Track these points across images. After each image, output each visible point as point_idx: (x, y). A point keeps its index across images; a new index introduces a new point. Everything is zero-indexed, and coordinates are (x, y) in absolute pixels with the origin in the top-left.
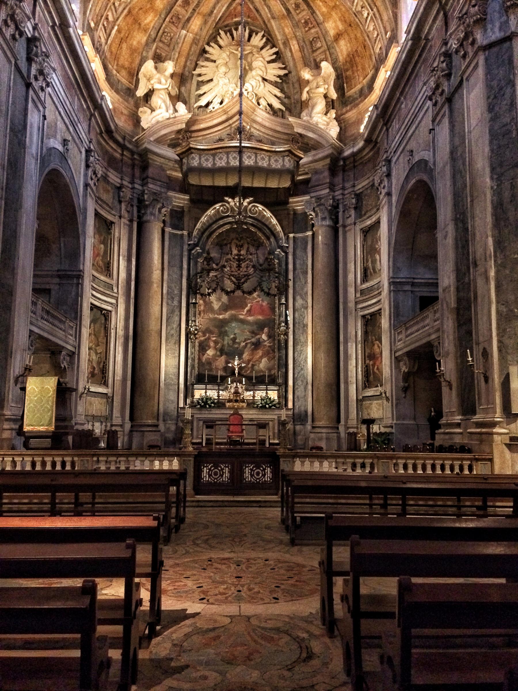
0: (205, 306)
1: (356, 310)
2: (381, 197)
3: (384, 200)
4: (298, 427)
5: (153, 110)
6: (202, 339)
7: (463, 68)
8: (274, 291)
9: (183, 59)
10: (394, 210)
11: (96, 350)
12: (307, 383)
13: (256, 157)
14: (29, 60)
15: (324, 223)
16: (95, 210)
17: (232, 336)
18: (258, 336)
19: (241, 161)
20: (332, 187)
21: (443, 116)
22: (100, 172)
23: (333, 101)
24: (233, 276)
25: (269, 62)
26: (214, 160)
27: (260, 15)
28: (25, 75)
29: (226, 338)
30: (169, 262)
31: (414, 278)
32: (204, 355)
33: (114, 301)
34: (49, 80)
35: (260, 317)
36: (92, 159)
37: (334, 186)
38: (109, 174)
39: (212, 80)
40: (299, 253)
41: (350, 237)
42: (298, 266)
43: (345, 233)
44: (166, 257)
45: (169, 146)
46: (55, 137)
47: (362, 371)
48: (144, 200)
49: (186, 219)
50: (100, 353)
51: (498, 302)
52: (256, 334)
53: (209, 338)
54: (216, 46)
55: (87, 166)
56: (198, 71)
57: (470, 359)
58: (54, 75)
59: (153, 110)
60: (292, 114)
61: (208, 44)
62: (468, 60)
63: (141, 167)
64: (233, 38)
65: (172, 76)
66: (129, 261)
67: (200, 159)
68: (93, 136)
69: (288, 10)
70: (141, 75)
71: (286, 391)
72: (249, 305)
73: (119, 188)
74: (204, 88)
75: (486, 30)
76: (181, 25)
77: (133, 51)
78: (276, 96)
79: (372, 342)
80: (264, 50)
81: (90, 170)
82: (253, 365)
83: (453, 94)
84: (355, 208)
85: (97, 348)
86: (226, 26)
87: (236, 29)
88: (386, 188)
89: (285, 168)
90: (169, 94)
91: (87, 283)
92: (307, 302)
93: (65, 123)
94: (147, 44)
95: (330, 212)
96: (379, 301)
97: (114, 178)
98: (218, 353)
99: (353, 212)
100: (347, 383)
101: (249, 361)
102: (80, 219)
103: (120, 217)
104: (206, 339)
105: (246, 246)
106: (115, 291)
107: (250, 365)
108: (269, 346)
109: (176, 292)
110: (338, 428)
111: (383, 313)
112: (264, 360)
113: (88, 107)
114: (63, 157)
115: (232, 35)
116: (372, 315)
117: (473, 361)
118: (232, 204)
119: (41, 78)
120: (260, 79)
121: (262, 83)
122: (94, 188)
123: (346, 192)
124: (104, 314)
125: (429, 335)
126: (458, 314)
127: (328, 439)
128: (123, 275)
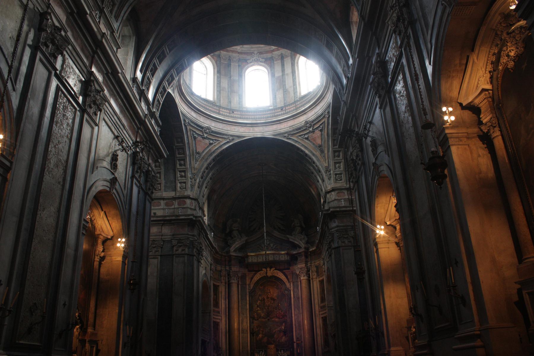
1: (319, 315)
6: (257, 330)
17: (269, 328)
18: (281, 327)
30: (241, 298)
33: (220, 318)
36: (212, 267)
37: (307, 262)
41: (315, 283)
42: (295, 296)
43: (313, 282)
44: (240, 296)
49: (247, 279)
55: (211, 270)
59: (232, 238)
67: (252, 259)
73: (221, 271)
82: (279, 340)
95: (307, 274)
96: (326, 312)
97: (219, 268)
99: (315, 273)
100: (317, 346)
103: (221, 283)
107: (278, 340)
113: (211, 249)
128: (223, 306)
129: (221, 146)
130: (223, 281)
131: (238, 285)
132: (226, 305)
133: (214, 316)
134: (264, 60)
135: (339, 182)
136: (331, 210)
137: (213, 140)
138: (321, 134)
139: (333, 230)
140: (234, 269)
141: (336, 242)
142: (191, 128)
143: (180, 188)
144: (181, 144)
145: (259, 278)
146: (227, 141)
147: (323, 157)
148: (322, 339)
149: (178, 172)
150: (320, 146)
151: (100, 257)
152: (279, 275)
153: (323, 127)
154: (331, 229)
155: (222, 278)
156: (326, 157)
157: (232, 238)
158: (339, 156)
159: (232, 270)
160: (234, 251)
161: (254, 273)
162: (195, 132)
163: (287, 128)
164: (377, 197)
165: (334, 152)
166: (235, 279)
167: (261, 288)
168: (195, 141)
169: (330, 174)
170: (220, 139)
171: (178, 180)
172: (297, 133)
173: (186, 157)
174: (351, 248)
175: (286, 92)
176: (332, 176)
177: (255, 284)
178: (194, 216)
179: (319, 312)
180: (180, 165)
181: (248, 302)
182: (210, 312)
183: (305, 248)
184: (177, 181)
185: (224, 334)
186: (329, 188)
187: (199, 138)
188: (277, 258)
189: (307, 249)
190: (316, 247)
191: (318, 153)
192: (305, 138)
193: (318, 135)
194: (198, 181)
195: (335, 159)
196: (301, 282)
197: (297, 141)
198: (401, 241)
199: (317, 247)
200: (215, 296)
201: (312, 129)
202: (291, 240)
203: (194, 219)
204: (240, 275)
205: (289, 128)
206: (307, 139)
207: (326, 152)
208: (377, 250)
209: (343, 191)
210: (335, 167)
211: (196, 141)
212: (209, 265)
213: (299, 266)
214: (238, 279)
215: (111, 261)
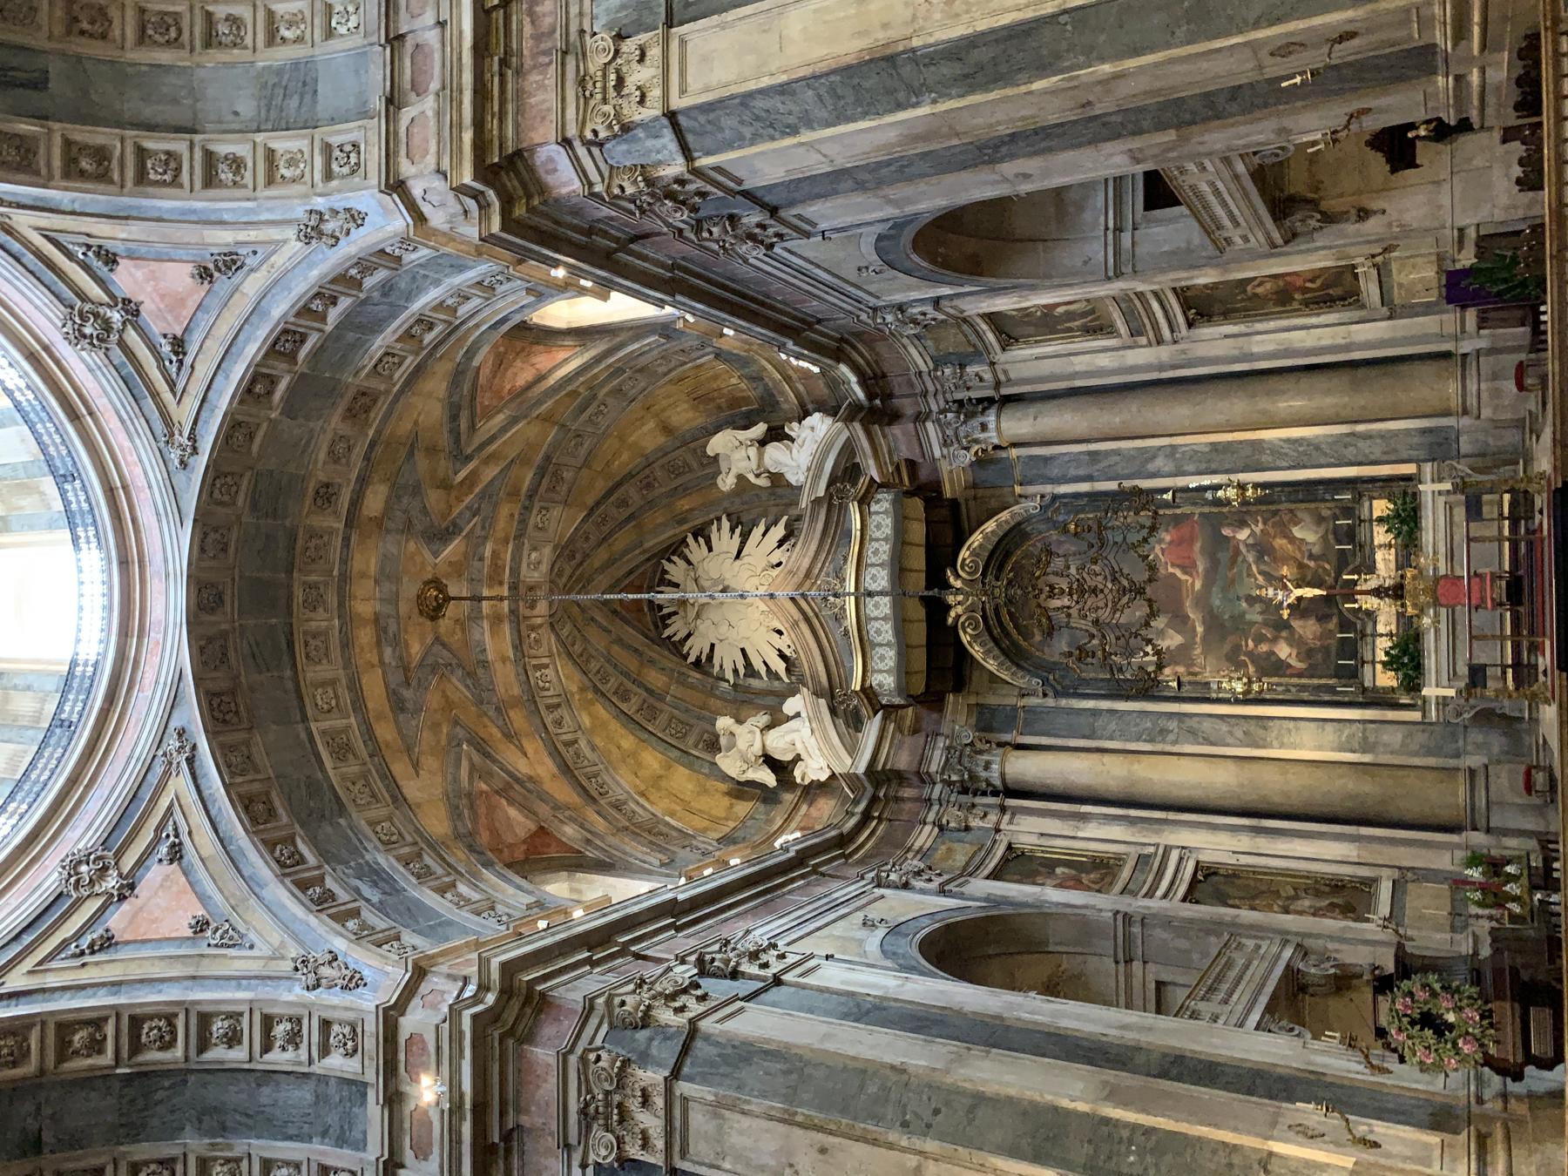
0: (1177, 663)
2: (941, 317)
4: (1465, 446)
5: (798, 758)
6: (1251, 669)
7: (721, 194)
8: (1145, 517)
9: (712, 701)
10: (967, 289)
11: (1288, 898)
12: (1353, 434)
13: (873, 565)
14: (735, 974)
15: (992, 426)
16: (987, 878)
18: (1243, 548)
19: (881, 593)
20: (920, 418)
21: (799, 217)
22: (915, 862)
23: (769, 429)
24: (1115, 604)
25: (710, 550)
26: (881, 645)
27: (637, 567)
28: (762, 984)
29: (1248, 617)
30: (1084, 737)
31: (1107, 229)
32: (1289, 666)
33: (1175, 855)
34: (766, 944)
35: (1197, 546)
36: (893, 877)
38: (917, 845)
39: (743, 650)
40: (1055, 472)
42: (1081, 472)
45: (858, 730)
46: (861, 942)
47: (1318, 315)
48: (962, 782)
49: (992, 700)
51: (1168, 46)
52: (1237, 552)
53: (1250, 654)
54: (689, 643)
55: (906, 886)
56: (729, 675)
57: (1298, 80)
58: (757, 933)
60: (795, 503)
61: (685, 657)
62: (709, 188)
63: (900, 785)
64: (675, 613)
65: (740, 722)
66: (1084, 817)
67: (881, 671)
68: (853, 872)
70: (743, 778)
71: (1373, 480)
72: (1171, 570)
73: (941, 828)
75: (660, 163)
76: (658, 705)
77: (704, 791)
78: (764, 535)
79: (1249, 299)
80: (690, 557)
81: (914, 882)
83: (763, 205)
84: (962, 366)
85: (1283, 894)
86: (657, 627)
87: (660, 608)
88: (923, 309)
90: (769, 727)
91: (1138, 905)
92: (1160, 448)
93: (834, 921)
94: (690, 767)
95: (970, 416)
96: (1155, 294)
97: (924, 836)
98: (1284, 634)
99: (971, 370)
100: (1348, 348)
102: (1009, 910)
103: (998, 831)
104: (1253, 662)
105: (1053, 579)
106: (1152, 850)
108: (1265, 523)
109: (1149, 725)
110: (1465, 356)
111: (1183, 284)
112: (1297, 532)
113: (802, 877)
114: (895, 930)
115: (670, 615)
116: (1186, 305)
117: (1300, 74)
118: (960, 609)
119: (764, 958)
120: (738, 562)
122: (946, 877)
123: (931, 388)
124: (1206, 877)
125: (1236, 177)
126: (1194, 123)
127: (1495, 377)
128: (1116, 832)
133: (1159, 893)
136: (467, 178)
137: (157, 840)
138: (131, 256)
139: (594, 176)
141: (650, 143)
142: (29, 963)
143: (350, 1054)
144: (110, 1030)
146: (184, 765)
147: (259, 257)
148: (1314, 320)
149: (268, 1057)
150: (204, 274)
153: (79, 245)
154: (591, 185)
155: (975, 823)
156: (252, 235)
157: (798, 758)
158: (237, 164)
162: (65, 944)
163: (136, 448)
165: (210, 180)
166: (986, 757)
168: (127, 943)
169: (335, 212)
170: (164, 803)
171: (310, 1062)
172: (155, 395)
173: (187, 1006)
174: (674, 45)
176: (338, 201)
178: (476, 999)
179: (1160, 341)
180: (233, 1039)
181: (1105, 704)
182: (1128, 918)
183: (849, 420)
184: (317, 1068)
185: (1264, 844)
187: (117, 920)
188: (880, 551)
189: (854, 413)
190: (838, 360)
191: (252, 285)
192: (176, 353)
193: (139, 274)
194: (340, 944)
195: (251, 186)
197: (203, 400)
199: (839, 355)
200: (1059, 870)
201: (109, 306)
202: (821, 493)
203: (490, 999)
204: (968, 735)
205: (137, 441)
206: (179, 345)
207: (224, 238)
211: (128, 937)
212: (882, 891)
213: (937, 454)
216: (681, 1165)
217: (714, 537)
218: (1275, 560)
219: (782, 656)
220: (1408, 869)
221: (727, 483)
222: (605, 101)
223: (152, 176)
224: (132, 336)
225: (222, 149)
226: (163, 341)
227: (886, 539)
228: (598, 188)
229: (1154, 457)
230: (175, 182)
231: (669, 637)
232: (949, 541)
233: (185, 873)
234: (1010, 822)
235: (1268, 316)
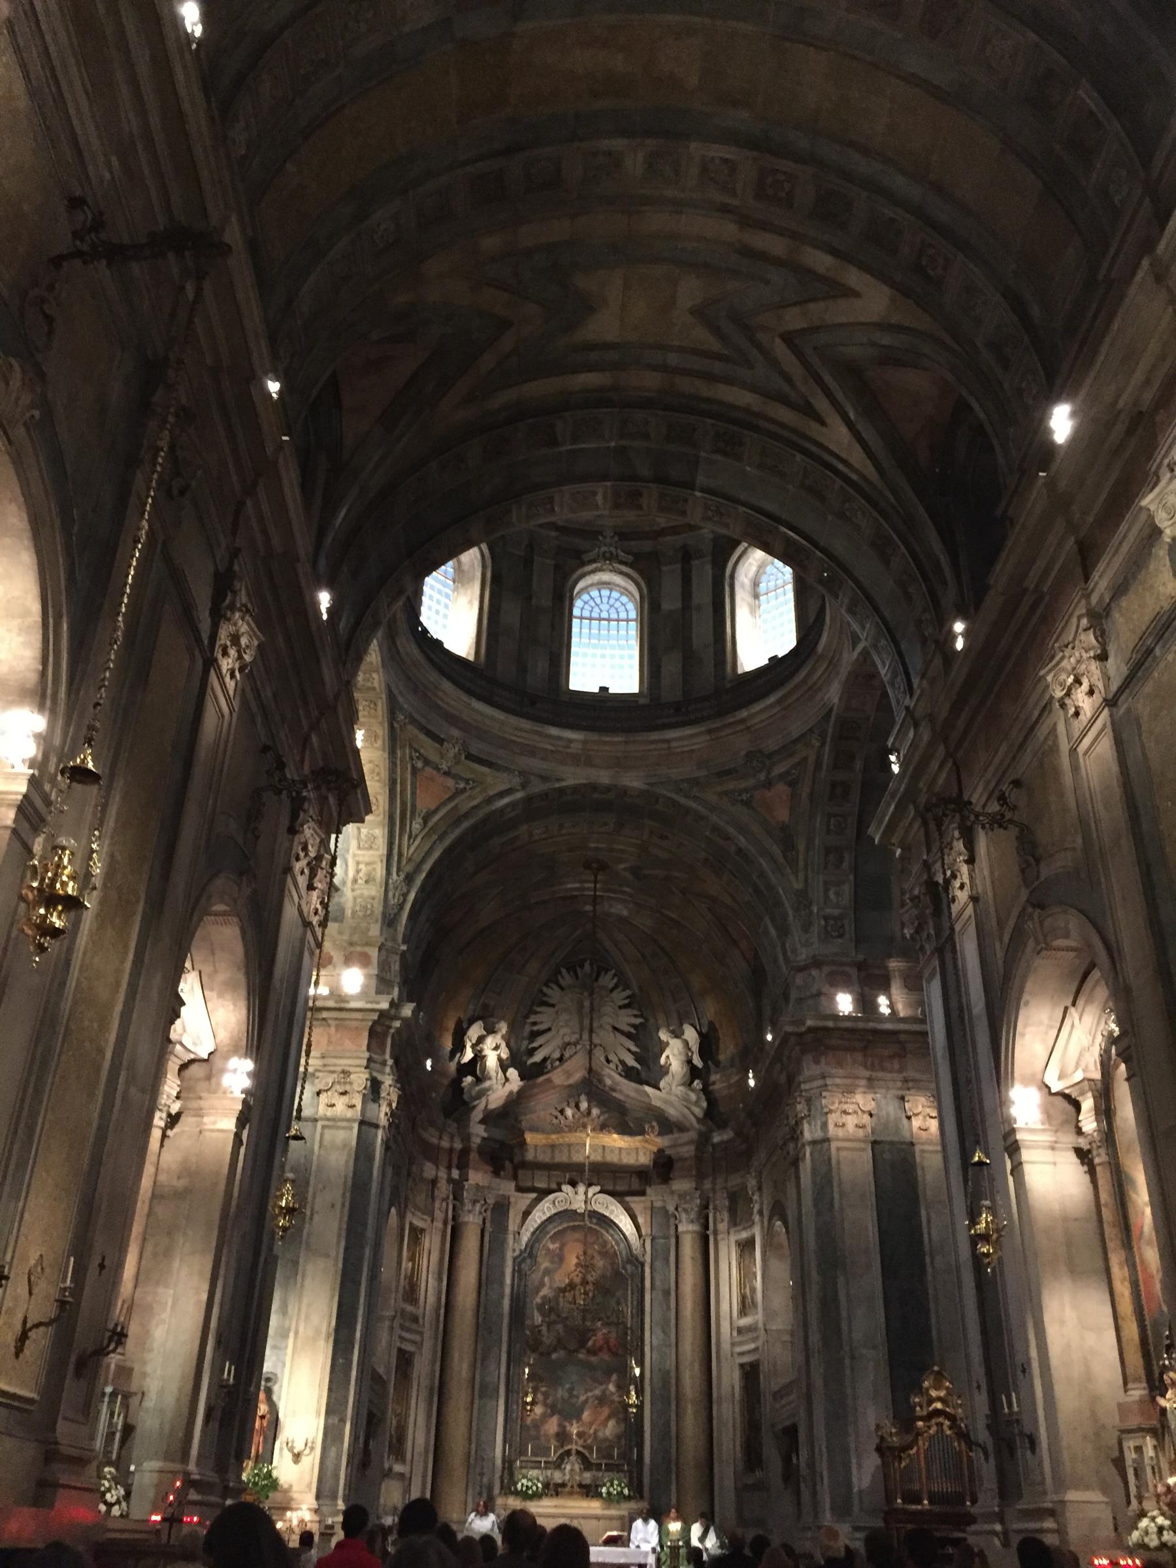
1: (732, 1356)
3: (756, 1218)
12: (670, 1461)
17: (567, 1386)
18: (603, 1387)
25: (620, 1007)
33: (417, 1338)
39: (549, 1029)
40: (658, 1264)
42: (658, 1283)
47: (741, 1446)
50: (400, 1414)
56: (533, 1018)
59: (479, 1080)
61: (546, 985)
66: (440, 1279)
69: (643, 956)
74: (540, 1041)
78: (629, 1050)
87: (582, 966)
89: (638, 1164)
95: (699, 1213)
96: (756, 1350)
99: (726, 1215)
101: (591, 1424)
103: (432, 1221)
107: (592, 1431)
112: (611, 1423)
120: (610, 1029)
121: (611, 1034)
128: (431, 1299)
129: (489, 800)
130: (439, 1215)
131: (483, 1231)
132: (439, 1299)
134: (630, 558)
135: (835, 940)
137: (467, 781)
140: (477, 1177)
145: (548, 1215)
148: (738, 1443)
150: (784, 828)
151: (169, 1115)
152: (612, 1212)
155: (437, 1204)
156: (801, 864)
159: (470, 1182)
160: (482, 1122)
161: (534, 1195)
164: (1027, 1003)
165: (828, 851)
167: (551, 1246)
174: (863, 1145)
175: (690, 658)
177: (533, 1233)
179: (733, 1344)
181: (507, 1290)
183: (701, 1134)
186: (803, 955)
191: (776, 851)
196: (677, 1238)
198: (1099, 1147)
204: (491, 1201)
206: (747, 803)
207: (801, 847)
208: (1017, 1168)
209: (847, 969)
210: (826, 897)
214: (485, 1211)
215: (201, 1132)
216: (319, 1124)
217: (629, 1011)
218: (596, 1407)
219: (545, 1060)
220: (410, 1485)
221: (663, 1035)
222: (840, 1103)
223: (833, 820)
224: (751, 782)
225: (847, 856)
226: (748, 795)
227: (620, 1159)
228: (803, 1087)
229: (664, 1332)
230: (828, 832)
231: (560, 973)
232: (619, 1188)
233: (451, 799)
234: (436, 1228)
235: (742, 1415)
